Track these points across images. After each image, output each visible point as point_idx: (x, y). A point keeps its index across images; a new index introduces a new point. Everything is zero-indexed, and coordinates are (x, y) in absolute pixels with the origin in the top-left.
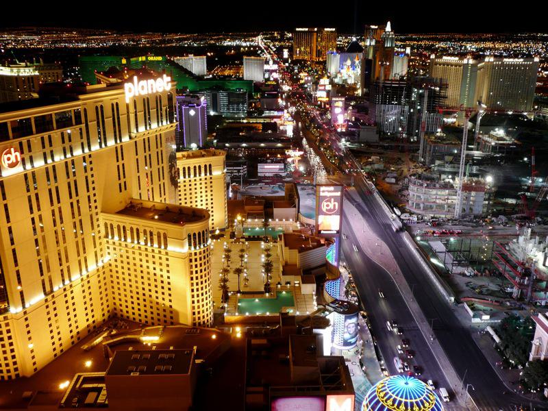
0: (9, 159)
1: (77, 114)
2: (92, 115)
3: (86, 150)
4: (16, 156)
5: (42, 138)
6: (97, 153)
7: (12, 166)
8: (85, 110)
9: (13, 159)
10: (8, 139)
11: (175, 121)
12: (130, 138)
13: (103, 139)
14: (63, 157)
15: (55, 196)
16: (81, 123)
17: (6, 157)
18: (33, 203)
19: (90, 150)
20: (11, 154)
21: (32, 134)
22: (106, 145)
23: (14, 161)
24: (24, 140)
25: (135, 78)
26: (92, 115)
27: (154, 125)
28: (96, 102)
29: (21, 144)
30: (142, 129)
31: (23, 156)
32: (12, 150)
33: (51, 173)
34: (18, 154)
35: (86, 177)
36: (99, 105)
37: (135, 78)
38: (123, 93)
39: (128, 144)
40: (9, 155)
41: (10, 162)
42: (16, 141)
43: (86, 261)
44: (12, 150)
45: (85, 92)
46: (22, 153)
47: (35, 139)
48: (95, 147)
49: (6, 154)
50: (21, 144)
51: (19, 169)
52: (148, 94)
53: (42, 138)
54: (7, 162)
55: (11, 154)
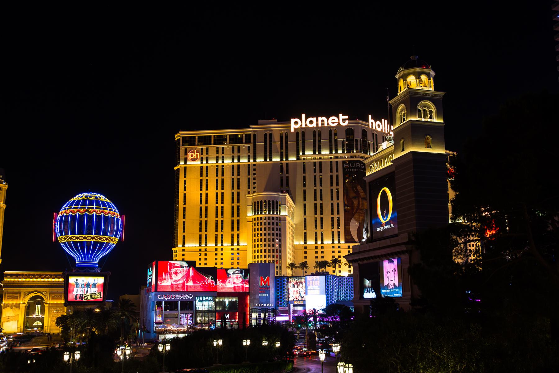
0: (192, 156)
1: (248, 137)
2: (260, 138)
3: (252, 160)
4: (197, 155)
5: (217, 148)
6: (261, 165)
7: (193, 160)
8: (255, 135)
9: (195, 156)
10: (194, 145)
11: (355, 152)
12: (298, 158)
13: (268, 154)
14: (230, 161)
15: (219, 184)
16: (250, 143)
17: (190, 154)
18: (204, 185)
19: (255, 161)
20: (194, 153)
21: (210, 144)
22: (271, 160)
23: (195, 157)
24: (205, 147)
25: (303, 116)
26: (260, 138)
27: (325, 152)
28: (265, 131)
29: (202, 149)
30: (309, 152)
31: (202, 156)
32: (195, 151)
33: (220, 171)
34: (198, 153)
35: (249, 179)
36: (268, 133)
37: (303, 116)
38: (290, 127)
39: (293, 163)
40: (192, 154)
41: (192, 157)
42: (199, 147)
43: (238, 237)
44: (195, 151)
45: (257, 124)
46: (202, 154)
47: (212, 148)
48: (260, 160)
49: (191, 153)
50: (202, 149)
51: (198, 162)
52: (317, 127)
53: (217, 148)
54: (190, 157)
55: (194, 153)
